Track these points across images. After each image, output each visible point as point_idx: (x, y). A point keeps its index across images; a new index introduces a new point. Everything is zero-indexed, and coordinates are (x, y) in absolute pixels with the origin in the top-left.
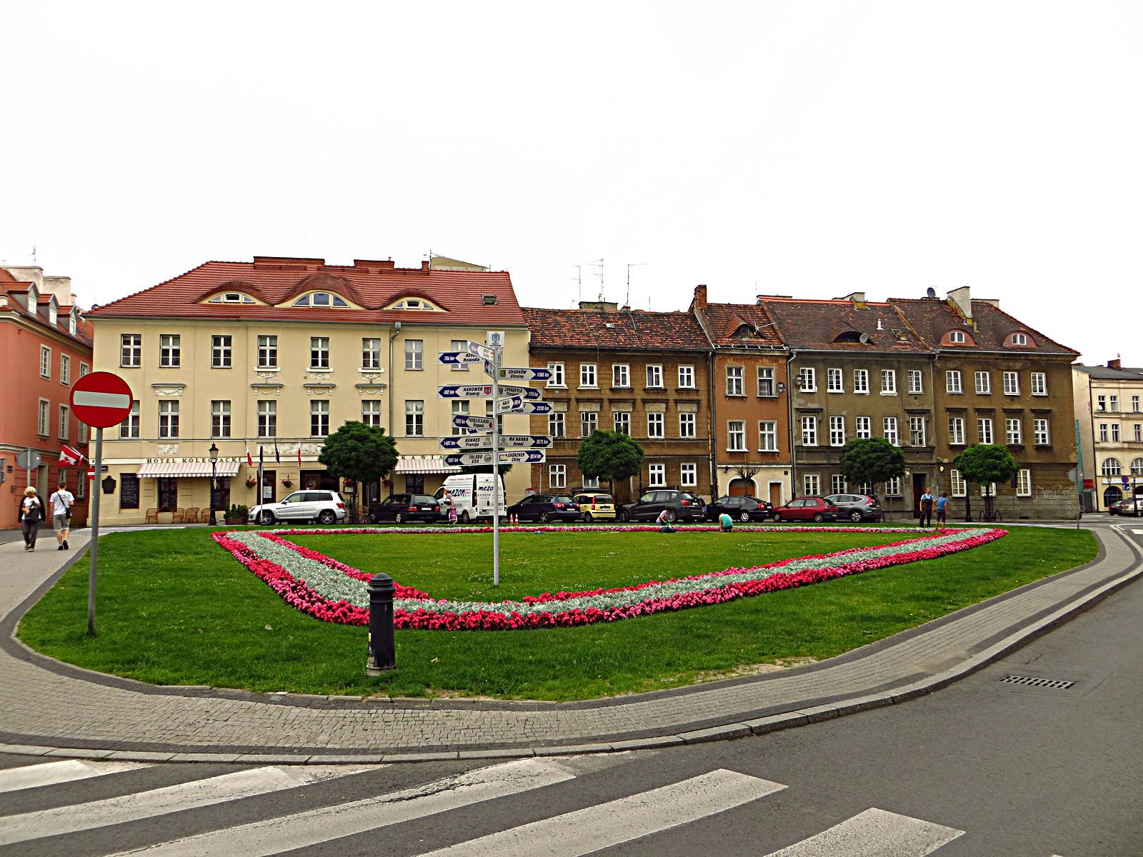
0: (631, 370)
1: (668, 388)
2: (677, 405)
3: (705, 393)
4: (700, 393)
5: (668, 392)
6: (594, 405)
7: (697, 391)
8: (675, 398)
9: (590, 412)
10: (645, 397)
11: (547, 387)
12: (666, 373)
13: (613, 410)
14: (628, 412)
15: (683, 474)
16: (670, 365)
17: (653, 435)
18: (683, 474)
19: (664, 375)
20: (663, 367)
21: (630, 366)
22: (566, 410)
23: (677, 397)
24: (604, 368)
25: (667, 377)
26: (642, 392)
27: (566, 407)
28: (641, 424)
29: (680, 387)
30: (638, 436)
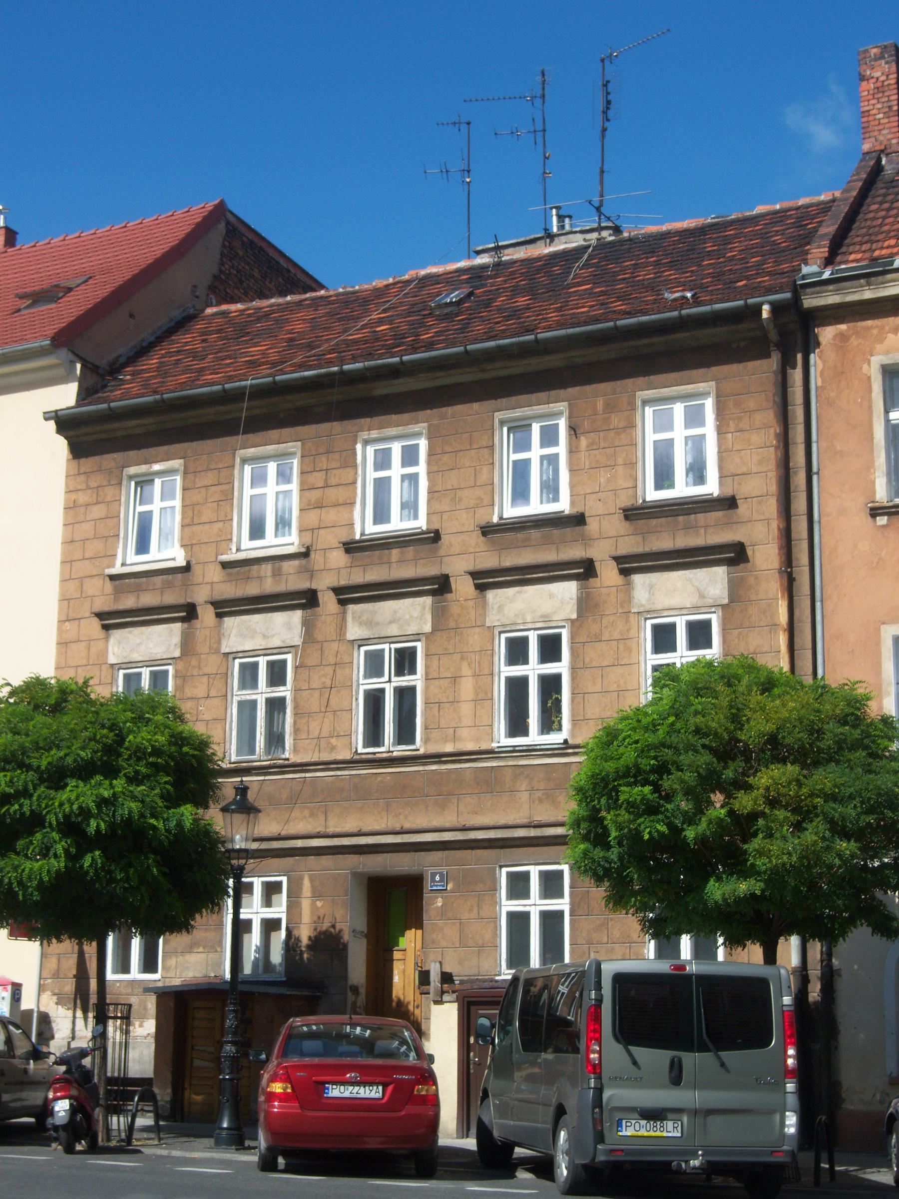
0: (431, 453)
1: (592, 508)
2: (629, 585)
3: (771, 507)
4: (743, 508)
5: (592, 525)
6: (279, 618)
7: (729, 503)
8: (622, 551)
9: (267, 652)
10: (489, 561)
11: (117, 569)
12: (584, 442)
13: (354, 632)
14: (417, 637)
15: (512, 916)
16: (600, 404)
17: (525, 732)
18: (512, 916)
19: (572, 451)
20: (570, 417)
21: (430, 439)
22: (177, 654)
23: (630, 546)
24: (323, 462)
25: (583, 456)
26: (476, 540)
27: (176, 639)
28: (467, 687)
29: (653, 495)
30: (455, 739)
